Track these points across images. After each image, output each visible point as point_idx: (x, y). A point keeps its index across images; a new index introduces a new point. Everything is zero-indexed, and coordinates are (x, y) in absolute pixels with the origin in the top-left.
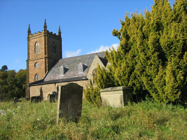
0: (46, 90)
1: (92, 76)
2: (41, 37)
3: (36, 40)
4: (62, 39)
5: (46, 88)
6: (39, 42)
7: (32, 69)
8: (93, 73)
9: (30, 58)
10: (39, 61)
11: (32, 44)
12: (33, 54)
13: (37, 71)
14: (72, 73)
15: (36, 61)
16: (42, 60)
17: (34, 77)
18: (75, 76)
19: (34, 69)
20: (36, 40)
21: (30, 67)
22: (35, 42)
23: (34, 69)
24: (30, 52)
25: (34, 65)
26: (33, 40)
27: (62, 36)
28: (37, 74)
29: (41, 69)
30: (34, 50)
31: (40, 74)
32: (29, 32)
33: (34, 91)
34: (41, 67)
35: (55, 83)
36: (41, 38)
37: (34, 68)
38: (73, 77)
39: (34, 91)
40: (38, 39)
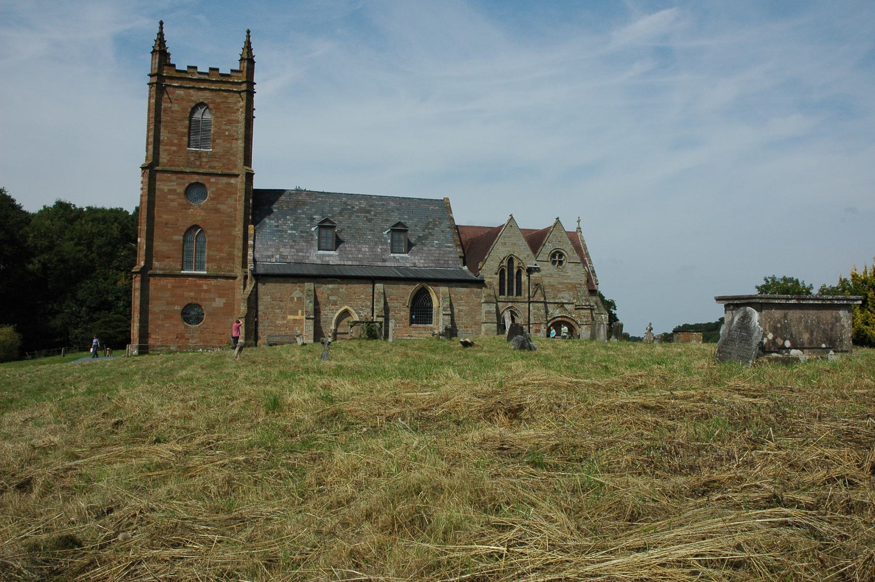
0: (331, 298)
1: (496, 274)
3: (198, 96)
7: (175, 204)
9: (164, 158)
11: (176, 107)
12: (179, 145)
13: (197, 212)
14: (365, 249)
15: (195, 178)
16: (225, 180)
17: (179, 238)
18: (384, 261)
19: (180, 204)
20: (198, 96)
21: (157, 193)
22: (193, 104)
23: (186, 207)
24: (164, 135)
25: (181, 190)
26: (181, 92)
28: (195, 227)
29: (217, 211)
30: (186, 130)
31: (210, 232)
32: (161, 52)
33: (278, 295)
34: (223, 207)
36: (226, 97)
37: (184, 201)
38: (380, 264)
39: (278, 295)
40: (207, 94)
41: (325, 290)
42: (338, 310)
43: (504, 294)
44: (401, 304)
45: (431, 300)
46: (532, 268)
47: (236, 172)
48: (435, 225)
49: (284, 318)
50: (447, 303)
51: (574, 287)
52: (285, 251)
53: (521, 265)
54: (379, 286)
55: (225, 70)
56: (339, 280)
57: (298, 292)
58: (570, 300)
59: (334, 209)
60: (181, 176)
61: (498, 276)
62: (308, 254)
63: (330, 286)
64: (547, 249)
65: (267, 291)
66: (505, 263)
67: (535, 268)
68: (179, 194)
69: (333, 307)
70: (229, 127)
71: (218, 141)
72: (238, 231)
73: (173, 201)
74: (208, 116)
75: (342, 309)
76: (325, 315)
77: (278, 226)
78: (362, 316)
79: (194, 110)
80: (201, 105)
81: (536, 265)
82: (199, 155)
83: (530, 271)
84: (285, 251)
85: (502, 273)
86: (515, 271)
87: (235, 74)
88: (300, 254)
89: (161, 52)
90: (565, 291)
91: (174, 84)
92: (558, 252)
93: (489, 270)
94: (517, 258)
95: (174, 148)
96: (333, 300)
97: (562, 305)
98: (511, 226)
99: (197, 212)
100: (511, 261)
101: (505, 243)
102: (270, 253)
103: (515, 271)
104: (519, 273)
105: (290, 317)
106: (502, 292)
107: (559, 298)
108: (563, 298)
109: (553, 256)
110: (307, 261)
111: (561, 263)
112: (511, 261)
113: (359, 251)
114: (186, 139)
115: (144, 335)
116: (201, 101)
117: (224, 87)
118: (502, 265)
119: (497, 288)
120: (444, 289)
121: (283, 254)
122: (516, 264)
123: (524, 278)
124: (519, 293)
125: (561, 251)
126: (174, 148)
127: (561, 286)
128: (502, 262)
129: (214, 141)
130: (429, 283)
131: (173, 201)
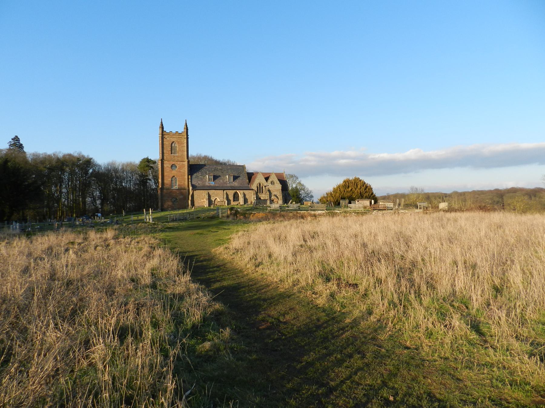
2: (180, 139)
3: (173, 140)
5: (213, 193)
6: (178, 143)
11: (167, 143)
14: (221, 181)
15: (173, 163)
16: (182, 163)
24: (165, 151)
25: (170, 166)
26: (168, 139)
28: (174, 176)
29: (180, 172)
30: (170, 150)
34: (181, 171)
35: (224, 190)
36: (181, 140)
37: (171, 169)
41: (211, 192)
45: (239, 195)
48: (241, 173)
49: (201, 200)
51: (277, 190)
52: (199, 182)
54: (225, 191)
57: (204, 193)
64: (270, 181)
65: (196, 193)
68: (169, 167)
72: (186, 177)
73: (168, 169)
82: (174, 156)
84: (199, 182)
85: (258, 187)
87: (183, 133)
93: (254, 186)
95: (167, 155)
99: (174, 172)
100: (260, 184)
105: (202, 200)
109: (272, 182)
111: (274, 184)
113: (220, 181)
115: (162, 206)
117: (180, 137)
120: (242, 191)
123: (264, 188)
124: (262, 192)
126: (167, 155)
129: (178, 152)
131: (168, 169)
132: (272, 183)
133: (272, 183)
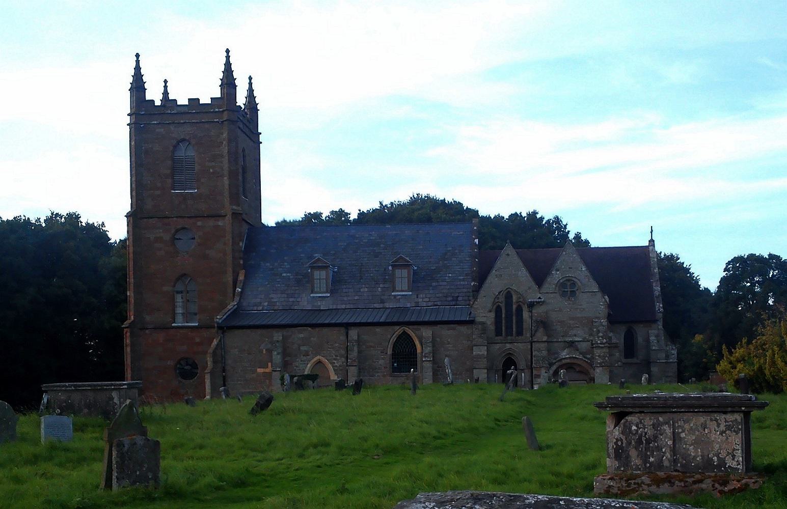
2: (207, 126)
4: (262, 138)
8: (494, 303)
10: (199, 223)
16: (211, 223)
22: (175, 142)
26: (161, 130)
27: (263, 125)
30: (168, 172)
32: (138, 86)
42: (310, 361)
43: (501, 335)
44: (379, 352)
46: (534, 302)
47: (223, 212)
50: (429, 348)
53: (521, 300)
54: (353, 333)
55: (205, 100)
56: (310, 329)
58: (585, 338)
59: (339, 244)
60: (166, 221)
61: (493, 315)
62: (299, 300)
63: (301, 336)
66: (502, 299)
67: (538, 303)
69: (305, 358)
70: (213, 164)
71: (203, 180)
74: (191, 153)
75: (315, 359)
76: (296, 367)
77: (272, 269)
78: (336, 366)
79: (175, 147)
80: (183, 140)
81: (540, 298)
82: (184, 197)
83: (531, 305)
84: (275, 297)
85: (498, 311)
86: (514, 307)
88: (291, 300)
89: (138, 86)
90: (578, 327)
91: (152, 123)
92: (569, 280)
94: (515, 291)
95: (158, 192)
96: (305, 350)
97: (571, 344)
98: (508, 255)
100: (509, 296)
101: (501, 275)
102: (258, 300)
103: (514, 307)
104: (519, 310)
105: (260, 370)
106: (498, 332)
107: (570, 336)
108: (575, 336)
110: (296, 308)
111: (573, 293)
112: (509, 296)
114: (169, 181)
116: (182, 137)
118: (497, 300)
119: (492, 328)
120: (427, 332)
121: (273, 300)
122: (514, 298)
123: (526, 315)
124: (520, 333)
125: (573, 279)
126: (158, 192)
127: (571, 322)
128: (497, 297)
130: (410, 327)
132: (568, 289)
133: (568, 289)
